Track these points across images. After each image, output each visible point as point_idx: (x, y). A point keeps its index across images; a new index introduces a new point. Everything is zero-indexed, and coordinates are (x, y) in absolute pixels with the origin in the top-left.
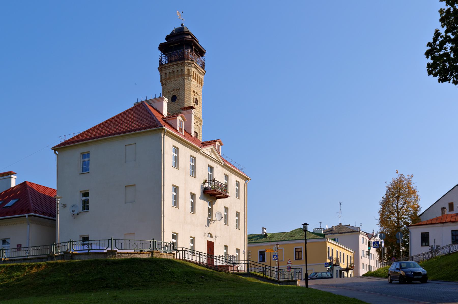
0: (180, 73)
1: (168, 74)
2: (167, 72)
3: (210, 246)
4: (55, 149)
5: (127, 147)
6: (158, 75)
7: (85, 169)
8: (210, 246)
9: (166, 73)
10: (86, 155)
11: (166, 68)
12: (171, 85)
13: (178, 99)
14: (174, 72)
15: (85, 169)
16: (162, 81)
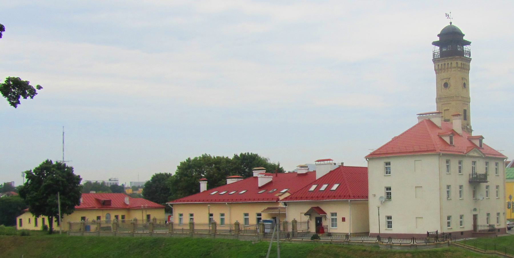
0: (450, 66)
1: (440, 65)
2: (440, 64)
3: (475, 217)
4: (366, 158)
5: (417, 162)
6: (432, 66)
7: (388, 172)
8: (475, 217)
9: (438, 65)
10: (388, 164)
11: (439, 61)
12: (444, 75)
13: (449, 85)
14: (445, 64)
15: (388, 172)
16: (435, 70)
